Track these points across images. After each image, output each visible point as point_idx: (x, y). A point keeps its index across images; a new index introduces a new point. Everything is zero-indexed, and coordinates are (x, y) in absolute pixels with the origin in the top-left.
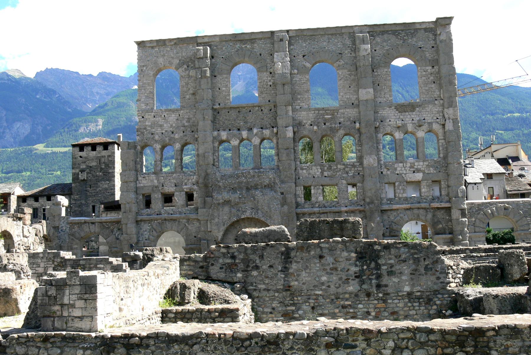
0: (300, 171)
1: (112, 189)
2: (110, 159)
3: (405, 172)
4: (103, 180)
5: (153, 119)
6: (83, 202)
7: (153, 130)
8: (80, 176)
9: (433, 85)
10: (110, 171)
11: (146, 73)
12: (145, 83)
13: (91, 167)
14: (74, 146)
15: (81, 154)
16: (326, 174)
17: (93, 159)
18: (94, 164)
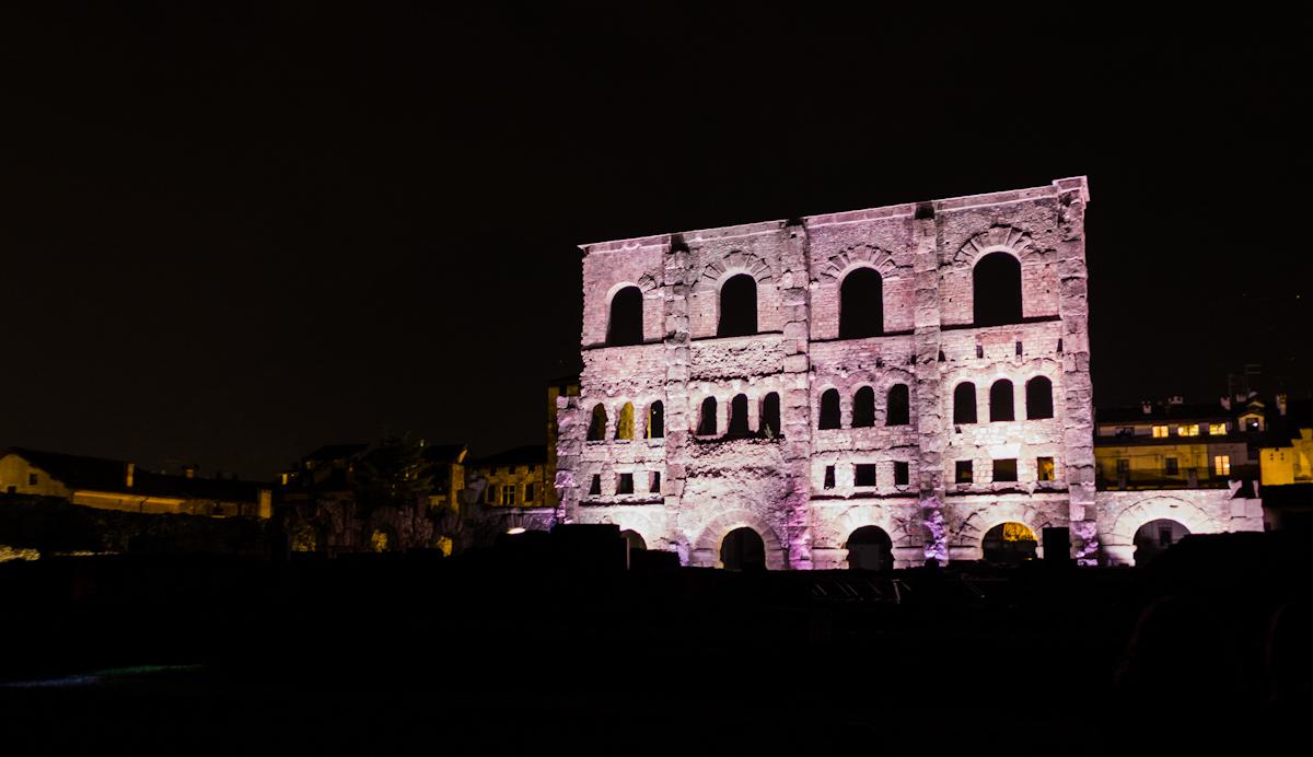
0: (819, 442)
3: (989, 442)
5: (603, 363)
7: (605, 379)
9: (1046, 296)
11: (596, 294)
12: (594, 309)
16: (859, 445)
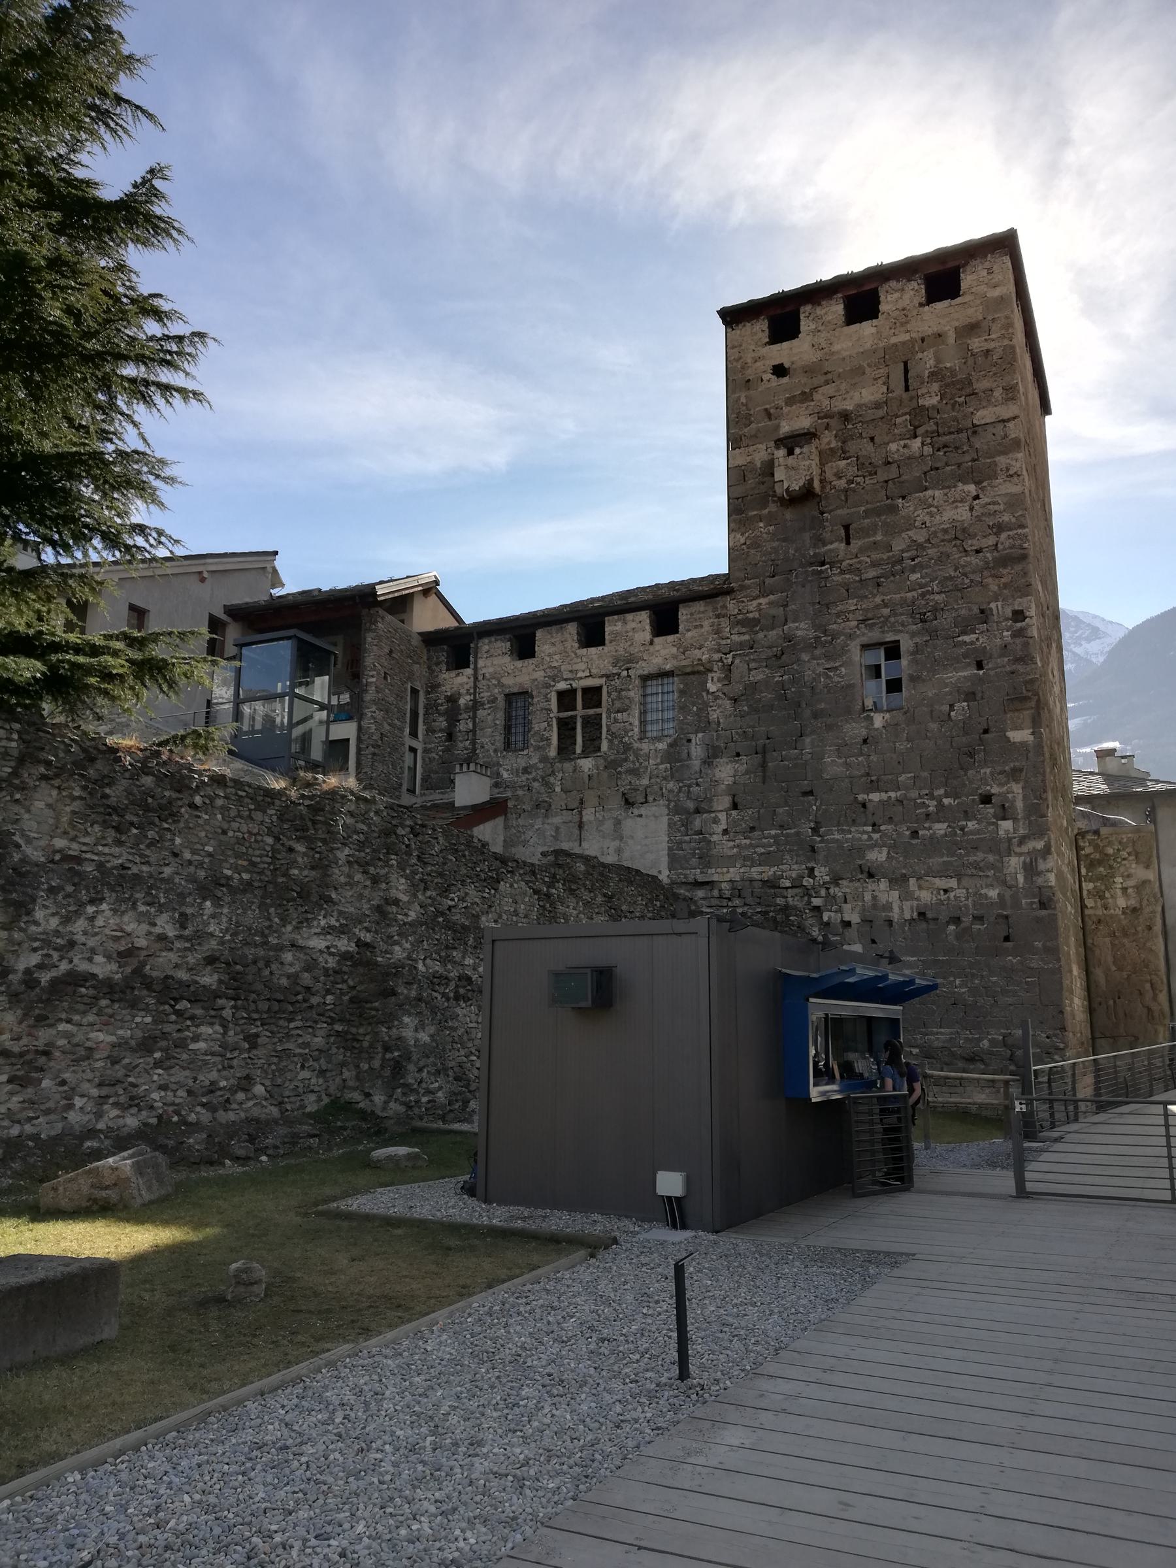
1: (999, 528)
2: (976, 344)
4: (933, 476)
6: (802, 629)
8: (779, 474)
10: (984, 415)
13: (845, 416)
14: (732, 317)
15: (782, 352)
17: (859, 371)
18: (869, 394)
